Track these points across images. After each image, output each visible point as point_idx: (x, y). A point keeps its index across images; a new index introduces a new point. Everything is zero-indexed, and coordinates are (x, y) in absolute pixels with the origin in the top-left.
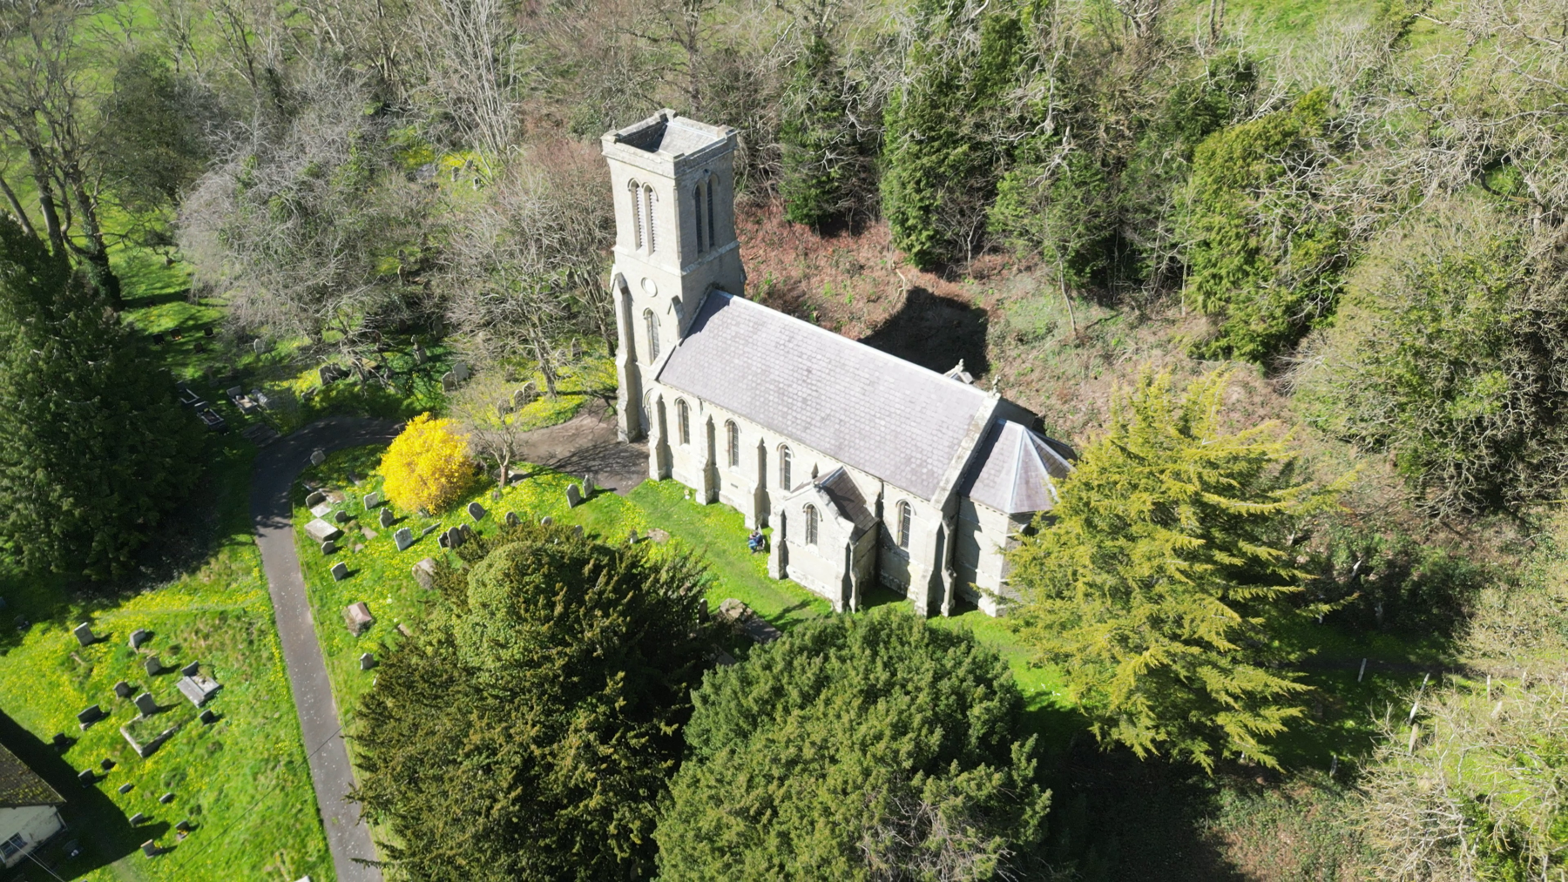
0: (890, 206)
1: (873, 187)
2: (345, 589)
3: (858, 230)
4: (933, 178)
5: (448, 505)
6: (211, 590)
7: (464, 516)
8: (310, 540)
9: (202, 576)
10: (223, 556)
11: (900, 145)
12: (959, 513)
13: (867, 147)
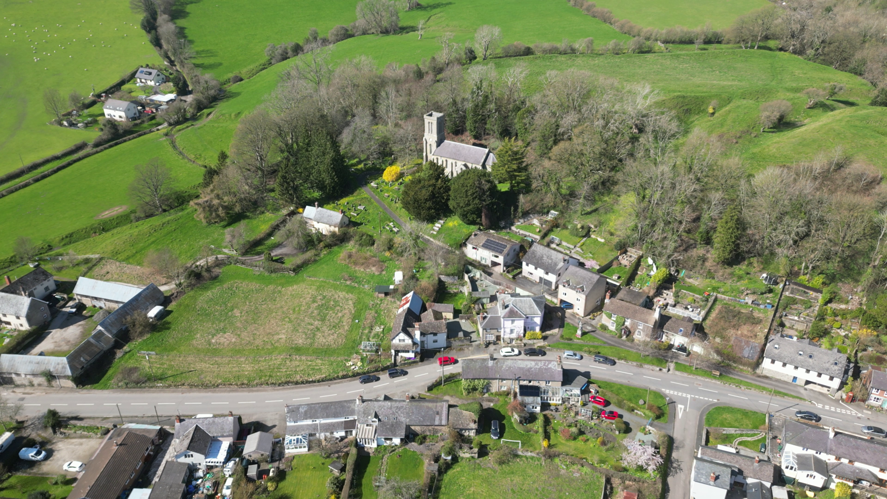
0: (468, 128)
1: (465, 124)
2: (383, 193)
3: (462, 134)
4: (475, 122)
5: (397, 180)
6: (358, 195)
7: (401, 180)
8: (373, 187)
9: (355, 194)
10: (358, 191)
11: (470, 116)
12: (484, 166)
13: (464, 118)
